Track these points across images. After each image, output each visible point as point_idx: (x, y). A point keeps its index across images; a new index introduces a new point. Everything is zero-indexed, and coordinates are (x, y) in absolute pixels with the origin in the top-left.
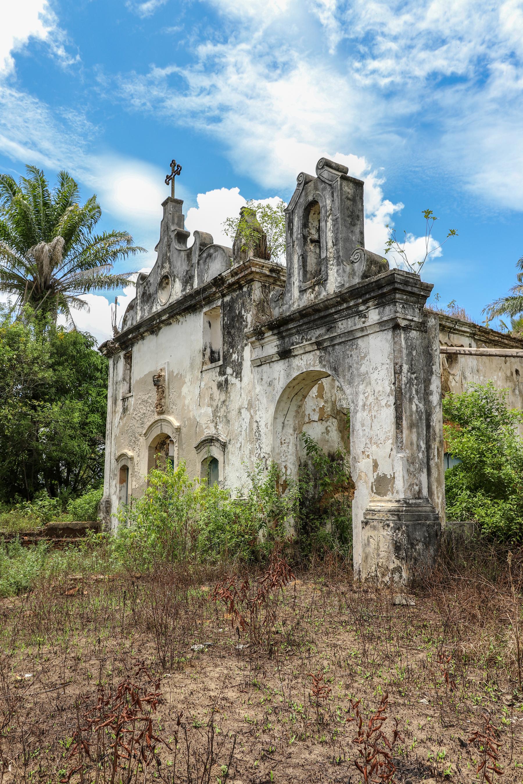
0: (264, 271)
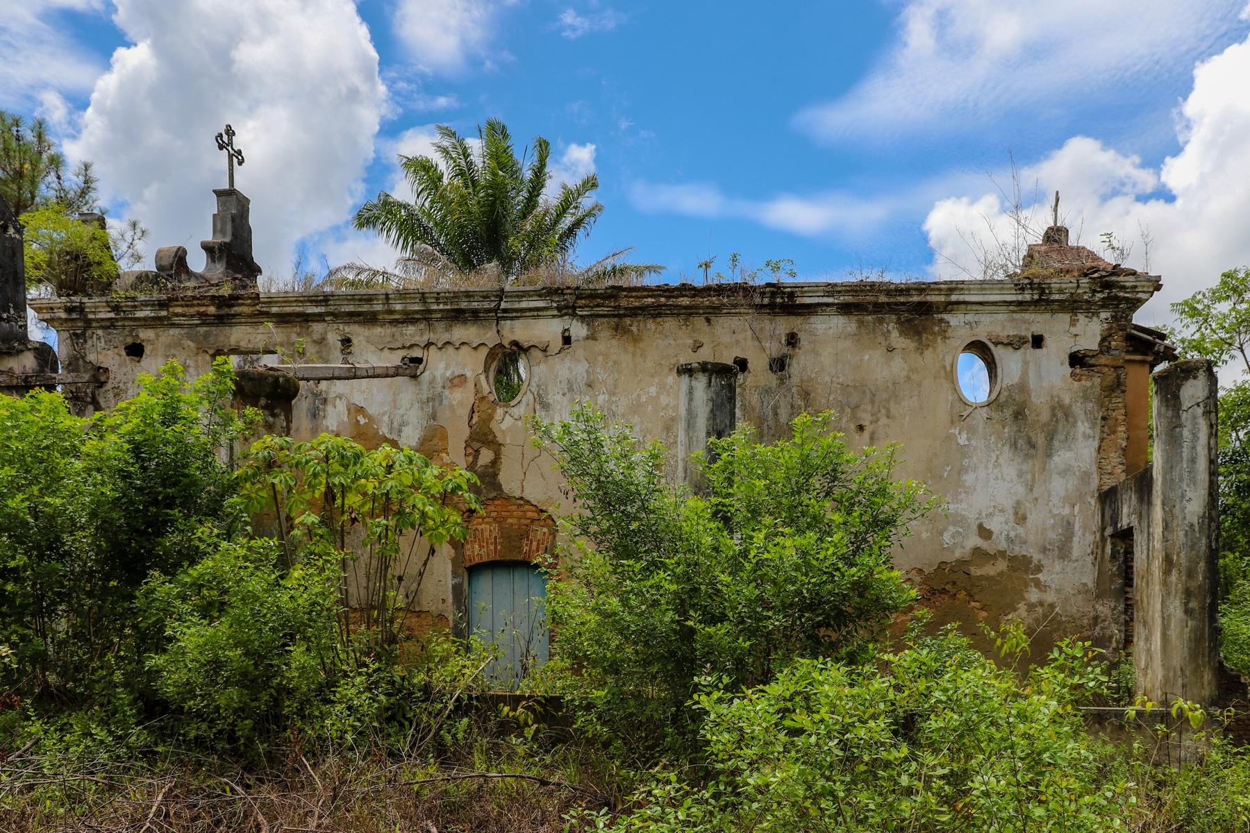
0: (57, 315)
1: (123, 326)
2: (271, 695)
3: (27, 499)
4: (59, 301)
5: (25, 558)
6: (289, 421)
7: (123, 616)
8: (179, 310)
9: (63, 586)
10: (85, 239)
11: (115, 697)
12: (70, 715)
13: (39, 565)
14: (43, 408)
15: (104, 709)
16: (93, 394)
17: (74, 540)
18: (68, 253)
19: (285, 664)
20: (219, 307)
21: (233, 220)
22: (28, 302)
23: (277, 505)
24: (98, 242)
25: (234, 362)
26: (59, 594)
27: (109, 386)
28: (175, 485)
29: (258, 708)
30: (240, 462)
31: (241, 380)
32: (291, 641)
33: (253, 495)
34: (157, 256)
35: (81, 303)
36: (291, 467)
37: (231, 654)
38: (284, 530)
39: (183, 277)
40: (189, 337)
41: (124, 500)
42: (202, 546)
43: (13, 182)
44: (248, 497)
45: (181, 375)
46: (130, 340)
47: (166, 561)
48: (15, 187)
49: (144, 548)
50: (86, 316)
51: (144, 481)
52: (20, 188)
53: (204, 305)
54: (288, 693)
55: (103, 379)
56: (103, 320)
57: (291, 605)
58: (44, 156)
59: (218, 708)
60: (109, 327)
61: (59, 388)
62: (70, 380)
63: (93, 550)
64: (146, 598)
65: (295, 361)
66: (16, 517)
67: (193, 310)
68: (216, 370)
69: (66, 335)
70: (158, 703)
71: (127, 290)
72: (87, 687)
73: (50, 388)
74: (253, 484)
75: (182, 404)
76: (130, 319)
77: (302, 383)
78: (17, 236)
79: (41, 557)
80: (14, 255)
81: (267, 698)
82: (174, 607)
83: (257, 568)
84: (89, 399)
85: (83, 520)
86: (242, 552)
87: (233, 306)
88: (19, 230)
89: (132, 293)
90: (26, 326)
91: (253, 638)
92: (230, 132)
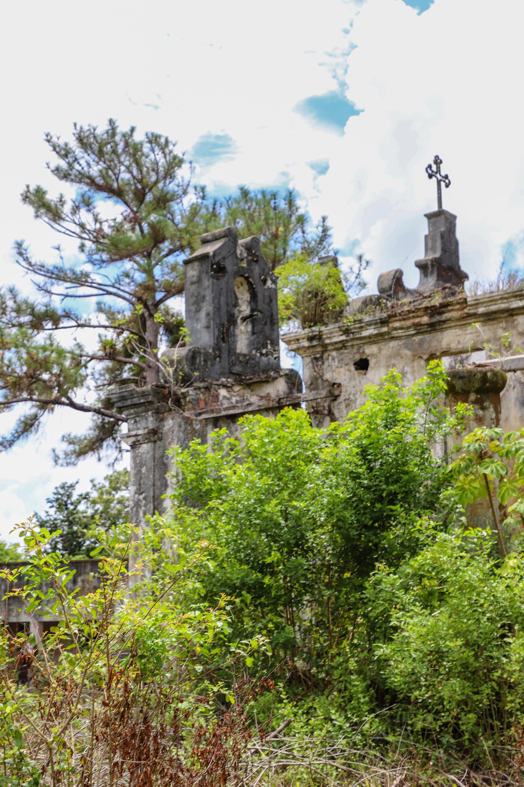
1: (352, 346)
2: (493, 689)
3: (280, 503)
4: (303, 332)
5: (279, 554)
6: (498, 412)
7: (354, 606)
8: (397, 324)
9: (306, 579)
10: (322, 278)
11: (350, 683)
12: (314, 700)
13: (288, 561)
14: (291, 424)
15: (342, 695)
16: (329, 407)
17: (316, 537)
18: (309, 293)
19: (505, 656)
20: (431, 316)
21: (442, 237)
22: (281, 337)
23: (489, 494)
24: (332, 279)
25: (446, 362)
26: (304, 586)
27: (341, 399)
28: (396, 481)
29: (481, 701)
30: (454, 456)
31: (452, 380)
32: (510, 631)
33: (467, 487)
34: (379, 281)
35: (320, 332)
36: (501, 456)
37: (452, 645)
38: (498, 519)
39: (401, 294)
40: (407, 347)
41: (354, 499)
42: (422, 538)
43: (271, 243)
44: (463, 489)
45: (399, 382)
46: (357, 357)
47: (391, 554)
48: (272, 247)
49: (372, 542)
50: (323, 342)
51: (370, 480)
52: (276, 247)
53: (418, 317)
54: (510, 687)
55: (336, 393)
56: (336, 343)
57: (507, 595)
58: (293, 218)
59: (441, 699)
60: (341, 348)
61: (304, 405)
62: (311, 398)
63: (330, 545)
64: (375, 588)
65: (502, 355)
66: (271, 520)
67: (409, 323)
68: (430, 373)
69: (308, 360)
70: (387, 691)
71: (355, 315)
72: (327, 673)
73: (296, 406)
74: (467, 475)
75: (401, 408)
76: (358, 339)
77: (509, 375)
78: (273, 286)
79: (290, 553)
80: (271, 301)
81: (488, 691)
82: (398, 597)
83: (472, 557)
84: (326, 412)
85: (322, 519)
86: (458, 543)
87: (443, 313)
88: (274, 282)
89: (359, 316)
90: (278, 357)
91: (472, 628)
92: (438, 161)
